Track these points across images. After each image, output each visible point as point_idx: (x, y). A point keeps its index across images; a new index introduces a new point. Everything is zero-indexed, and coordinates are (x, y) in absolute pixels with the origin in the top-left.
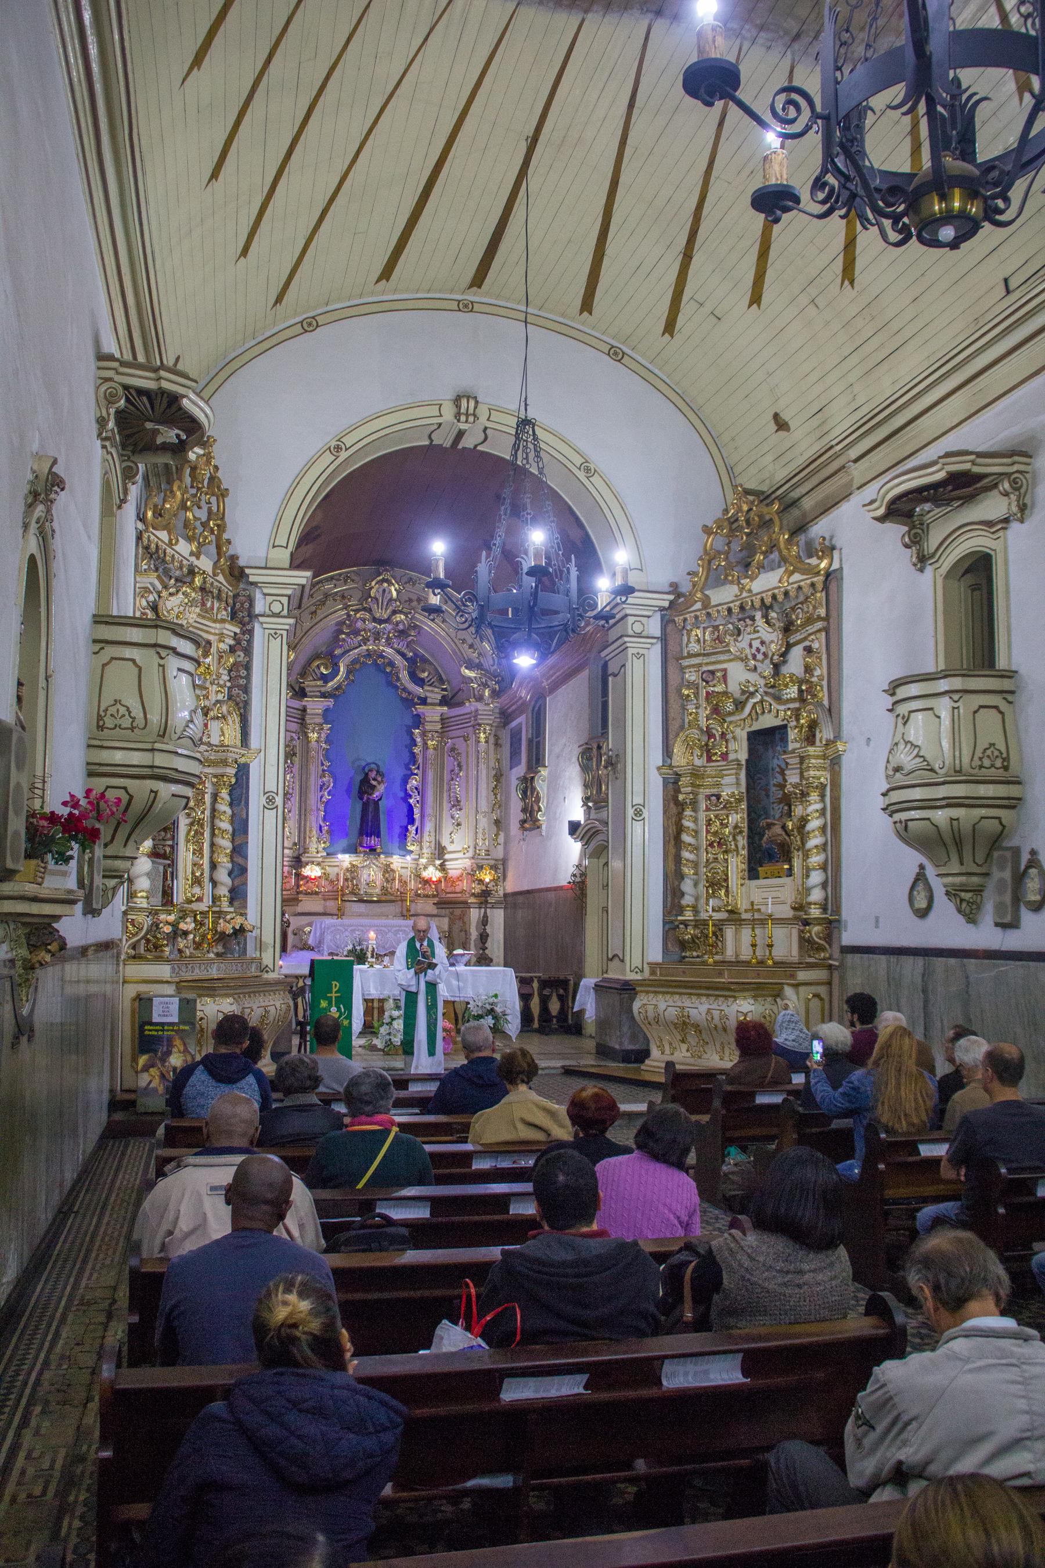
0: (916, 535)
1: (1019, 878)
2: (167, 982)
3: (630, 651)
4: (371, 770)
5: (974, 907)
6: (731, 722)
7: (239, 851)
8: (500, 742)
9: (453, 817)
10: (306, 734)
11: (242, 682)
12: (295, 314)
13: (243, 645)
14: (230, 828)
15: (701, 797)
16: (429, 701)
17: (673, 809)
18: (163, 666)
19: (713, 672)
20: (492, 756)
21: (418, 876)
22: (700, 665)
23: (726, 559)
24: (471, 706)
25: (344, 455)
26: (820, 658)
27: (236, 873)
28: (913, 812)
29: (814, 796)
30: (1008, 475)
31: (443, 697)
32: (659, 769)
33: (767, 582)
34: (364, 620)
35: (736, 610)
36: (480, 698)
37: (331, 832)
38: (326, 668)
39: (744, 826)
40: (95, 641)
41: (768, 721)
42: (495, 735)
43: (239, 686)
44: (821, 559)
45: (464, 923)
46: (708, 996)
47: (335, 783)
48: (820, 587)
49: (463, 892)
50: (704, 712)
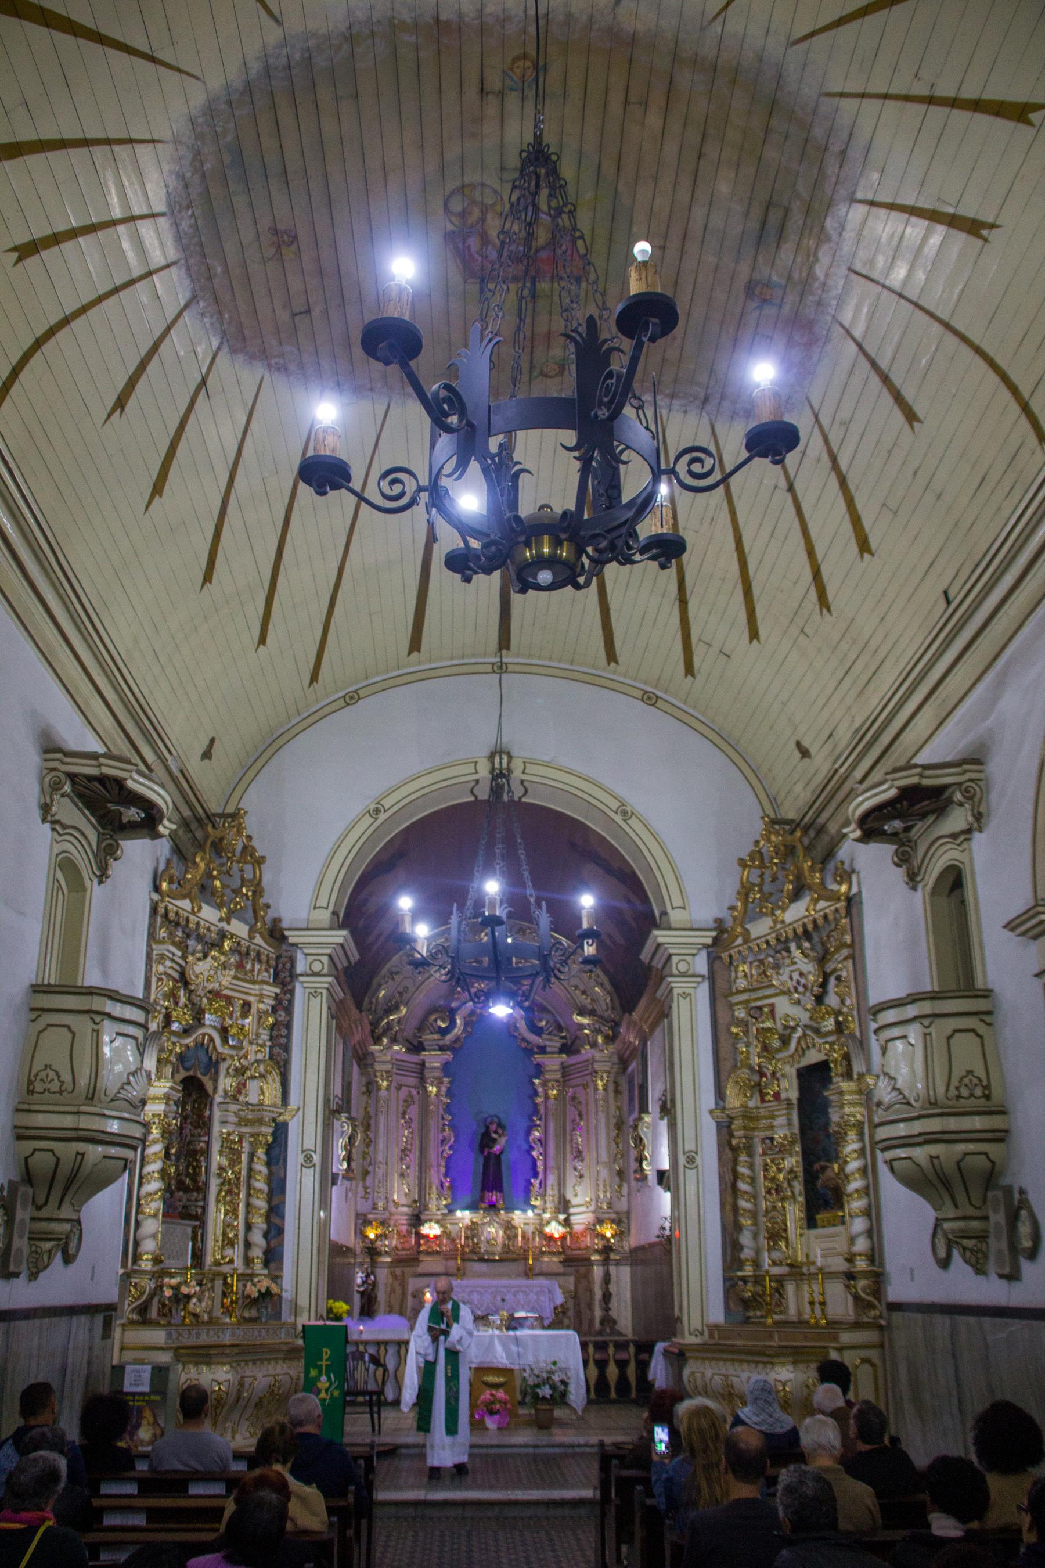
0: (904, 853)
1: (1013, 1219)
2: (162, 1349)
3: (676, 992)
5: (980, 1255)
6: (779, 1060)
7: (275, 1211)
9: (575, 1169)
10: (425, 1088)
11: (283, 1041)
12: (337, 691)
13: (283, 1005)
14: (265, 1188)
15: (757, 1141)
16: (548, 1049)
17: (729, 1154)
18: (98, 1031)
19: (760, 1008)
20: (611, 1101)
21: (541, 1232)
22: (748, 1001)
23: (761, 891)
24: (586, 1051)
25: (383, 817)
26: (849, 987)
27: (273, 1233)
28: (898, 1151)
29: (852, 1135)
30: (960, 784)
31: (563, 1045)
32: (711, 1112)
33: (796, 913)
35: (773, 942)
36: (594, 1045)
37: (452, 1187)
38: (443, 1021)
39: (800, 1170)
40: (32, 1010)
41: (813, 1057)
43: (280, 1046)
44: (840, 883)
46: (749, 1362)
48: (843, 912)
49: (587, 1248)
50: (756, 1049)
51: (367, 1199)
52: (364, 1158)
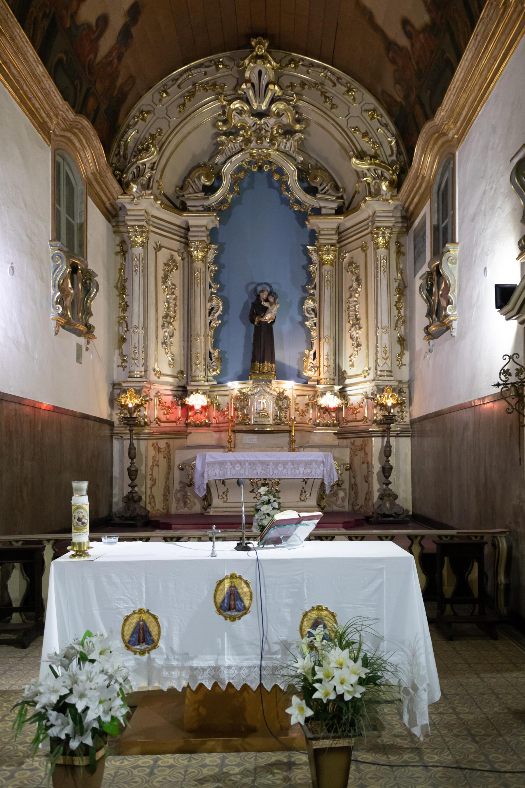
4: (262, 291)
8: (402, 249)
16: (323, 211)
34: (240, 112)
42: (397, 242)
45: (366, 454)
47: (223, 305)
49: (364, 419)
51: (124, 367)
52: (120, 324)
